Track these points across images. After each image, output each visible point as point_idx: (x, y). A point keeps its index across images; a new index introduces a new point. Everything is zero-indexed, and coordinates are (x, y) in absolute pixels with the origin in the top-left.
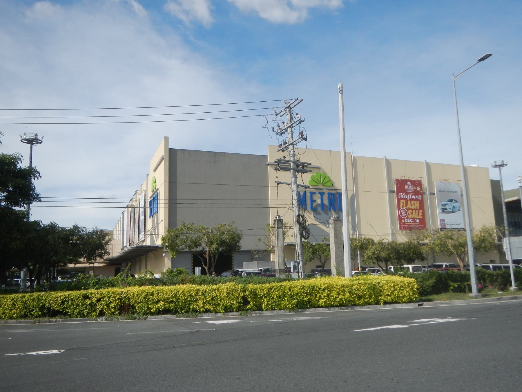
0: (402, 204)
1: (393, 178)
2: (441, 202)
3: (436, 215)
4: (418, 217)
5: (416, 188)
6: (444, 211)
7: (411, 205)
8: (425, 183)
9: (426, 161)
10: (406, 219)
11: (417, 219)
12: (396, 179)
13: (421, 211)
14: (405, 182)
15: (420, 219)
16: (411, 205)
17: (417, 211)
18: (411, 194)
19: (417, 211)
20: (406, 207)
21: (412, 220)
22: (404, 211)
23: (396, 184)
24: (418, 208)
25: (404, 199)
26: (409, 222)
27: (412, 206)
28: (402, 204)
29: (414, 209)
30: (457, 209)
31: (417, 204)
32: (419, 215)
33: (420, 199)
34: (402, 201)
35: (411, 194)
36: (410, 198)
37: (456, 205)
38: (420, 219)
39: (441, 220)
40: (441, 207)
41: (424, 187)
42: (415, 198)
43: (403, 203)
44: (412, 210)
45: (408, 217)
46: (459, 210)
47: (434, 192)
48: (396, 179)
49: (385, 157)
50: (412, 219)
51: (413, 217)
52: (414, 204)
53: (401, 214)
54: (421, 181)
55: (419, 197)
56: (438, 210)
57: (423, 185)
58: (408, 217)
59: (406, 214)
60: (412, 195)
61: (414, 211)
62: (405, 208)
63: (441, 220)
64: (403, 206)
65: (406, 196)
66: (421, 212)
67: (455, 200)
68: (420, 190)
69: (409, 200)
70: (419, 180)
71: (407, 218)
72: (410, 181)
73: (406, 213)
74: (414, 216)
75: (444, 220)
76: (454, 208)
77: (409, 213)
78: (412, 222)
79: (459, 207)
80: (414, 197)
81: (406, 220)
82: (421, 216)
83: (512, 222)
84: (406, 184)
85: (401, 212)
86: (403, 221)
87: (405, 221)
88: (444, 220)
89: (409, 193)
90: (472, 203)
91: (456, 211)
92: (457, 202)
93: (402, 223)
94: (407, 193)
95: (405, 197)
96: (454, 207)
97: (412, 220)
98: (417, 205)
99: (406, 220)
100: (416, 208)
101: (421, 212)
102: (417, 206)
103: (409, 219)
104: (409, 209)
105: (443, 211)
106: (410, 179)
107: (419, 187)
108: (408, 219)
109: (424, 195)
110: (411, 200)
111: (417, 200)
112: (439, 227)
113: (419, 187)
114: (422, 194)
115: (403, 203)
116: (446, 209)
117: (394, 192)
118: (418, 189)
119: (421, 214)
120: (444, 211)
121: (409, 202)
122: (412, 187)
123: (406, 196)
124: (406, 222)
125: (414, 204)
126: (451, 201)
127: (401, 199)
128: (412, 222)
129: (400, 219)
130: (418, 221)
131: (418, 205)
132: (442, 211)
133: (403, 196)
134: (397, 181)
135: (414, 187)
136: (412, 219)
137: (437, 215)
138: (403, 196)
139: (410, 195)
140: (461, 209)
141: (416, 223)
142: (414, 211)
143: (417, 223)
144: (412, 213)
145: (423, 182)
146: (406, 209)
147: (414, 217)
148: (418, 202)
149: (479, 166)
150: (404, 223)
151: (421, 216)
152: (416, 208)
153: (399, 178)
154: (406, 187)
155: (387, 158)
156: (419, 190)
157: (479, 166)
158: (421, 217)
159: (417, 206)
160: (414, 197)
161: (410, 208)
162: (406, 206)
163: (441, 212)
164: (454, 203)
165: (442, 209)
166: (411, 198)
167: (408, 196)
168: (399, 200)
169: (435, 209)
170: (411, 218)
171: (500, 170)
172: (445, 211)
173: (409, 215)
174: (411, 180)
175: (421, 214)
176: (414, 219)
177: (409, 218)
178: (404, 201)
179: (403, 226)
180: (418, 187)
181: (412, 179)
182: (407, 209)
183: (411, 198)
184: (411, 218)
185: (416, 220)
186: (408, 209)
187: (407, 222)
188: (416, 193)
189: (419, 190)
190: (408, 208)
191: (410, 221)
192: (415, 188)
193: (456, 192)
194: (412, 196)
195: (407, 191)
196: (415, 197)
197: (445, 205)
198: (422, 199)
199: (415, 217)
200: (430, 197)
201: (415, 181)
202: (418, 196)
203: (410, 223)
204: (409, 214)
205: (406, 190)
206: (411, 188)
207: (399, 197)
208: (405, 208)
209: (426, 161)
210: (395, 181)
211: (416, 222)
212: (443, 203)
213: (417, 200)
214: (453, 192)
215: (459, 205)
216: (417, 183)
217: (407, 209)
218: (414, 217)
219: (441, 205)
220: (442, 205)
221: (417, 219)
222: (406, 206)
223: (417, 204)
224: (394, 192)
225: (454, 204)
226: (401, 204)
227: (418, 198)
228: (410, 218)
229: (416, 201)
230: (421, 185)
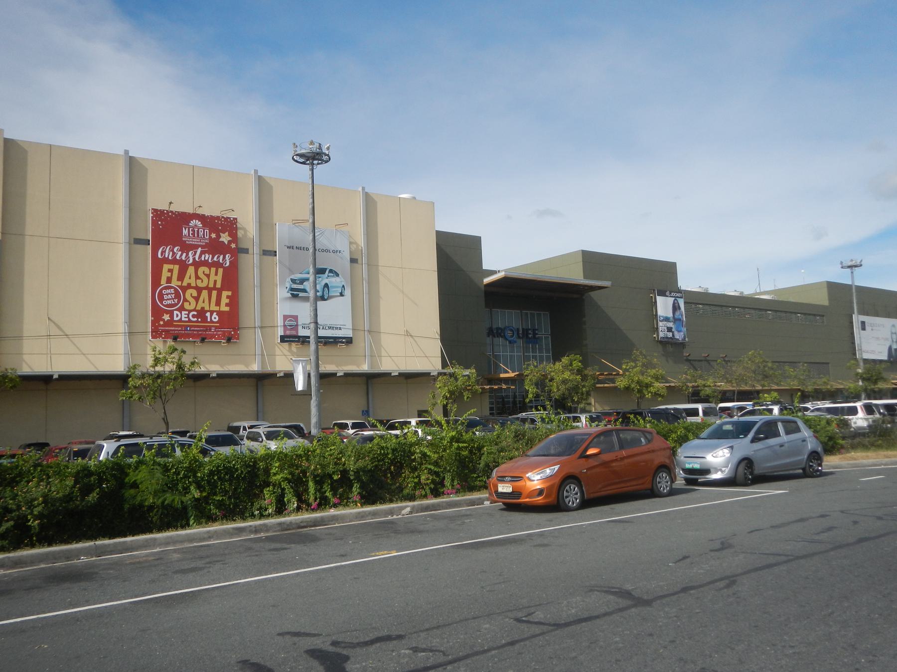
0: (169, 274)
1: (148, 209)
2: (292, 272)
3: (275, 304)
4: (214, 307)
5: (219, 237)
6: (296, 294)
7: (197, 277)
8: (248, 225)
9: (256, 171)
10: (175, 312)
11: (212, 313)
12: (152, 209)
13: (225, 294)
14: (185, 218)
15: (219, 313)
16: (197, 277)
17: (214, 293)
18: (200, 250)
19: (214, 293)
20: (179, 283)
21: (194, 316)
22: (172, 291)
23: (154, 223)
24: (219, 285)
25: (174, 261)
26: (187, 319)
27: (199, 281)
28: (169, 274)
29: (207, 288)
30: (335, 292)
31: (216, 274)
32: (218, 303)
33: (228, 264)
34: (166, 267)
35: (200, 250)
36: (194, 259)
37: (333, 281)
38: (219, 313)
39: (285, 317)
40: (288, 284)
41: (245, 235)
42: (210, 261)
43: (171, 271)
44: (199, 290)
45: (183, 304)
46: (342, 295)
47: (275, 250)
48: (152, 209)
49: (127, 152)
50: (195, 313)
51: (199, 308)
52: (208, 276)
53: (161, 298)
54: (236, 219)
55: (224, 257)
56: (282, 293)
57: (244, 229)
58: (183, 304)
59: (176, 301)
60: (202, 253)
61: (205, 293)
62: (175, 283)
63: (285, 317)
64: (169, 280)
65: (181, 255)
66: (228, 297)
67: (331, 271)
68: (230, 242)
69: (191, 265)
70: (230, 218)
71: (181, 309)
72: (201, 218)
73: (177, 295)
74: (203, 305)
75: (296, 318)
76: (326, 289)
77: (188, 296)
78: (195, 319)
79: (343, 286)
80: (207, 257)
81: (177, 316)
82: (227, 305)
83: (518, 330)
84: (187, 223)
85: (160, 293)
86: (166, 317)
87: (172, 316)
88: (296, 318)
89: (195, 247)
90: (382, 280)
91: (329, 298)
92: (337, 275)
93: (162, 323)
94: (186, 248)
95: (178, 257)
96: (326, 285)
97: (194, 316)
98: (217, 278)
99: (177, 316)
100: (211, 285)
101: (228, 297)
102: (215, 282)
103: (187, 312)
104: (189, 286)
105: (295, 296)
106: (200, 211)
107: (227, 233)
108: (183, 313)
109: (242, 257)
110: (197, 265)
111: (217, 265)
112: (280, 332)
113: (227, 233)
114: (238, 251)
115: (171, 271)
116: (304, 291)
117: (146, 242)
118: (225, 238)
119: (224, 301)
120: (296, 294)
121: (191, 270)
122: (206, 234)
123: (181, 255)
124: (175, 319)
125: (208, 276)
126: (321, 271)
127: (166, 261)
128: (195, 319)
129: (157, 312)
130: (215, 317)
131: (219, 279)
132: (291, 294)
133: (174, 253)
134: (158, 214)
135: (210, 234)
136: (195, 313)
137: (277, 303)
138: (174, 253)
139: (195, 253)
140: (348, 292)
141: (209, 322)
142: (205, 293)
143: (212, 322)
144: (197, 299)
145: (241, 222)
146: (177, 286)
147: (203, 308)
148: (221, 271)
149: (414, 198)
150: (170, 322)
151: (227, 305)
152: (211, 285)
153: (163, 206)
154: (185, 232)
155: (130, 155)
156: (226, 243)
157: (414, 198)
158: (227, 309)
159: (215, 282)
160: (207, 257)
161: (193, 285)
162: (181, 278)
163: (289, 298)
164: (327, 278)
165: (292, 289)
166: (197, 259)
167: (187, 254)
168: (157, 265)
169: (275, 288)
170: (194, 310)
171: (312, 170)
172: (301, 294)
173: (187, 301)
174: (204, 215)
175: (224, 301)
176: (201, 313)
177: (185, 310)
178: (176, 268)
179: (163, 331)
180: (224, 233)
181: (207, 211)
182: (180, 287)
183: (197, 257)
184: (194, 310)
185: (208, 314)
186: (184, 289)
187: (180, 320)
188: (215, 247)
189: (226, 243)
190: (185, 284)
191: (188, 317)
192: (213, 236)
193: (334, 252)
194: (203, 256)
195: (187, 242)
196: (213, 258)
197: (302, 281)
198: (234, 264)
199: (207, 308)
200: (261, 261)
201: (218, 218)
202: (221, 257)
203: (190, 321)
204: (185, 300)
205: (184, 239)
206: (201, 234)
207: (160, 256)
208: (175, 283)
209: (256, 171)
210: (151, 215)
211: (209, 320)
212: (298, 276)
213: (217, 265)
214: (327, 251)
215: (343, 283)
216: (222, 225)
217: (180, 287)
218: (203, 308)
219: (289, 280)
220: (293, 281)
221: (212, 313)
222: (181, 278)
223: (216, 274)
224: (146, 242)
225: (324, 279)
226: (165, 274)
227: (221, 261)
228: (190, 311)
229: (213, 270)
230: (236, 229)
